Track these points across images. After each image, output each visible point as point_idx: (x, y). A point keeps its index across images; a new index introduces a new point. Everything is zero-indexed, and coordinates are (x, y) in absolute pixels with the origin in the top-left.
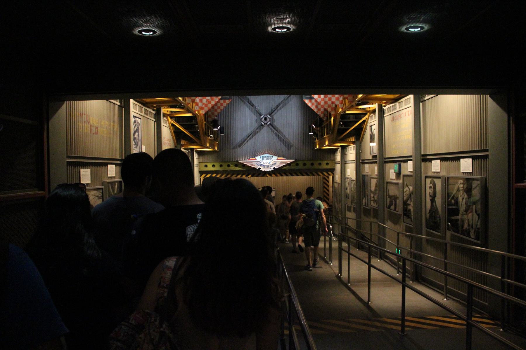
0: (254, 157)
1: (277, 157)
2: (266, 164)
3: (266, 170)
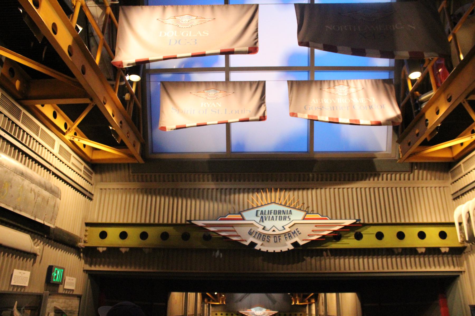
0: (240, 213)
1: (303, 214)
2: (271, 232)
3: (271, 250)
